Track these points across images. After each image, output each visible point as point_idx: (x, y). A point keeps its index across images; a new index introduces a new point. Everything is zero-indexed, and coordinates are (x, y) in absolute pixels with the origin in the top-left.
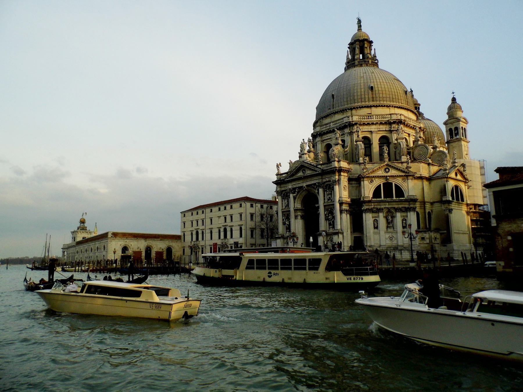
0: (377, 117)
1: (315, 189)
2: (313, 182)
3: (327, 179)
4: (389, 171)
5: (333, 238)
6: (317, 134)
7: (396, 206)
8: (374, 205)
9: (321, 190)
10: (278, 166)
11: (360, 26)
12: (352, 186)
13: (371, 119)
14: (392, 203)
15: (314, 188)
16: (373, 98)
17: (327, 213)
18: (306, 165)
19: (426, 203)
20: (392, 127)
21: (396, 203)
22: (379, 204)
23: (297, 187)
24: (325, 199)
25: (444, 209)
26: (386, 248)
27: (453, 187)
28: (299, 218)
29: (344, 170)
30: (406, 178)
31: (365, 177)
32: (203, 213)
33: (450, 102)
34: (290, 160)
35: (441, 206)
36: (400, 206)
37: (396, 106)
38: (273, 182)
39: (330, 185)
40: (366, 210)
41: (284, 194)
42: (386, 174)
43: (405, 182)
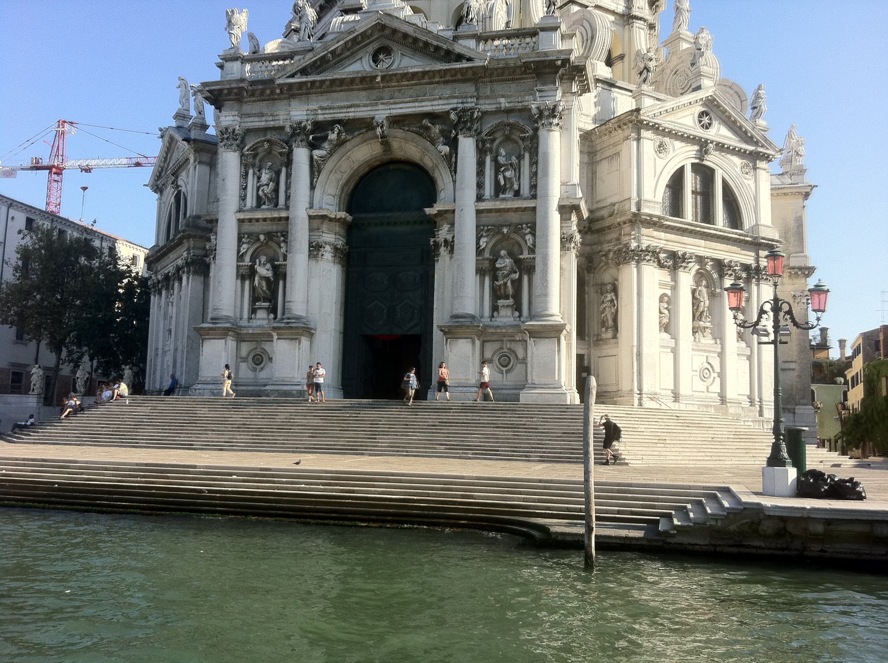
1: (433, 142)
2: (427, 107)
3: (502, 100)
4: (710, 124)
9: (467, 146)
15: (423, 132)
17: (487, 243)
23: (339, 121)
28: (328, 254)
39: (512, 126)
41: (254, 149)
42: (700, 132)
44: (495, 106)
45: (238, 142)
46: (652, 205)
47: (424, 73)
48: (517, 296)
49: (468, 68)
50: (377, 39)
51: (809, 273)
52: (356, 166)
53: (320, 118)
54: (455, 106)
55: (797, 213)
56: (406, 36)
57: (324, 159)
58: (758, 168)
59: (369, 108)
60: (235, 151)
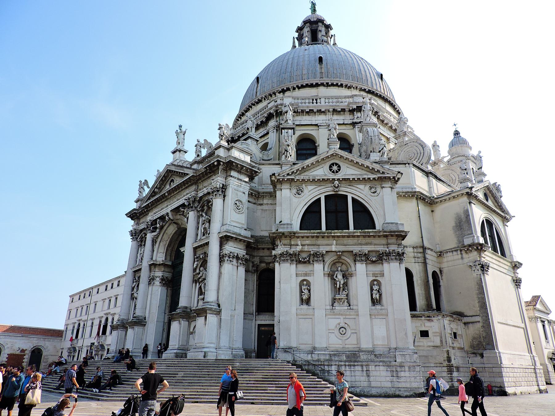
0: (327, 101)
3: (205, 189)
4: (339, 170)
7: (356, 249)
8: (302, 245)
9: (192, 215)
11: (314, 10)
12: (262, 210)
13: (317, 103)
14: (346, 241)
16: (321, 73)
17: (197, 265)
18: (173, 168)
19: (428, 252)
20: (356, 117)
21: (355, 241)
22: (313, 241)
24: (197, 235)
25: (469, 264)
26: (328, 357)
27: (483, 221)
28: (157, 282)
29: (237, 164)
30: (379, 186)
31: (283, 179)
32: (89, 295)
33: (452, 137)
34: (158, 171)
35: (462, 258)
36: (366, 249)
38: (126, 215)
40: (282, 255)
41: (142, 238)
42: (331, 176)
43: (376, 194)
44: (203, 193)
46: (286, 226)
51: (477, 248)
52: (171, 237)
55: (464, 208)
56: (175, 171)
58: (384, 187)
59: (166, 208)
60: (134, 241)
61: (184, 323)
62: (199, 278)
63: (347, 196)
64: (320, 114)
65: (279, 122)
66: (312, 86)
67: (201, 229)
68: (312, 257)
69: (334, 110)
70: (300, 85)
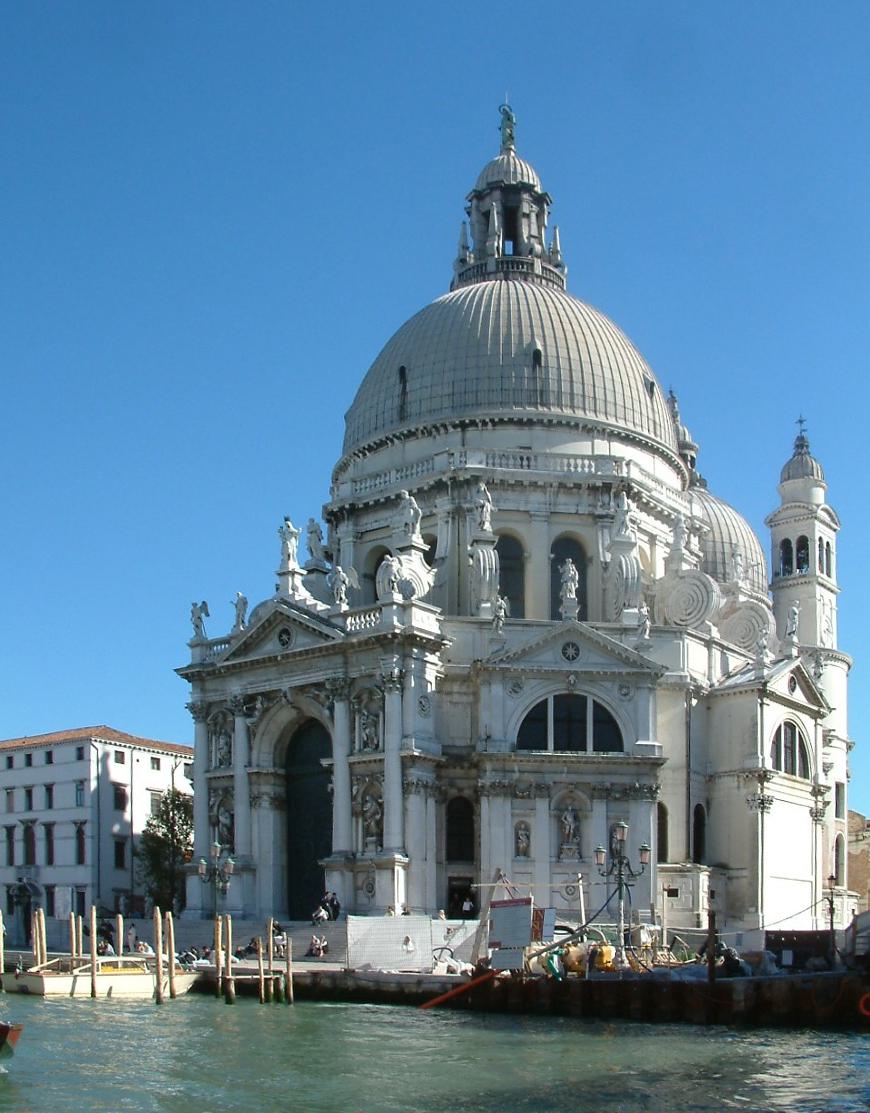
1: (323, 706)
4: (577, 655)
5: (374, 879)
6: (342, 509)
8: (520, 771)
9: (340, 708)
10: (201, 611)
13: (529, 466)
15: (316, 698)
23: (262, 694)
24: (353, 742)
28: (265, 803)
37: (616, 431)
40: (493, 785)
41: (215, 719)
42: (566, 667)
43: (628, 697)
45: (204, 714)
47: (307, 652)
48: (380, 835)
49: (333, 646)
50: (281, 621)
52: (282, 727)
53: (250, 692)
54: (328, 677)
56: (295, 620)
57: (256, 725)
60: (200, 722)
61: (349, 875)
62: (366, 811)
63: (584, 699)
64: (534, 491)
65: (457, 501)
66: (520, 423)
67: (360, 735)
68: (533, 790)
69: (560, 484)
70: (496, 420)
